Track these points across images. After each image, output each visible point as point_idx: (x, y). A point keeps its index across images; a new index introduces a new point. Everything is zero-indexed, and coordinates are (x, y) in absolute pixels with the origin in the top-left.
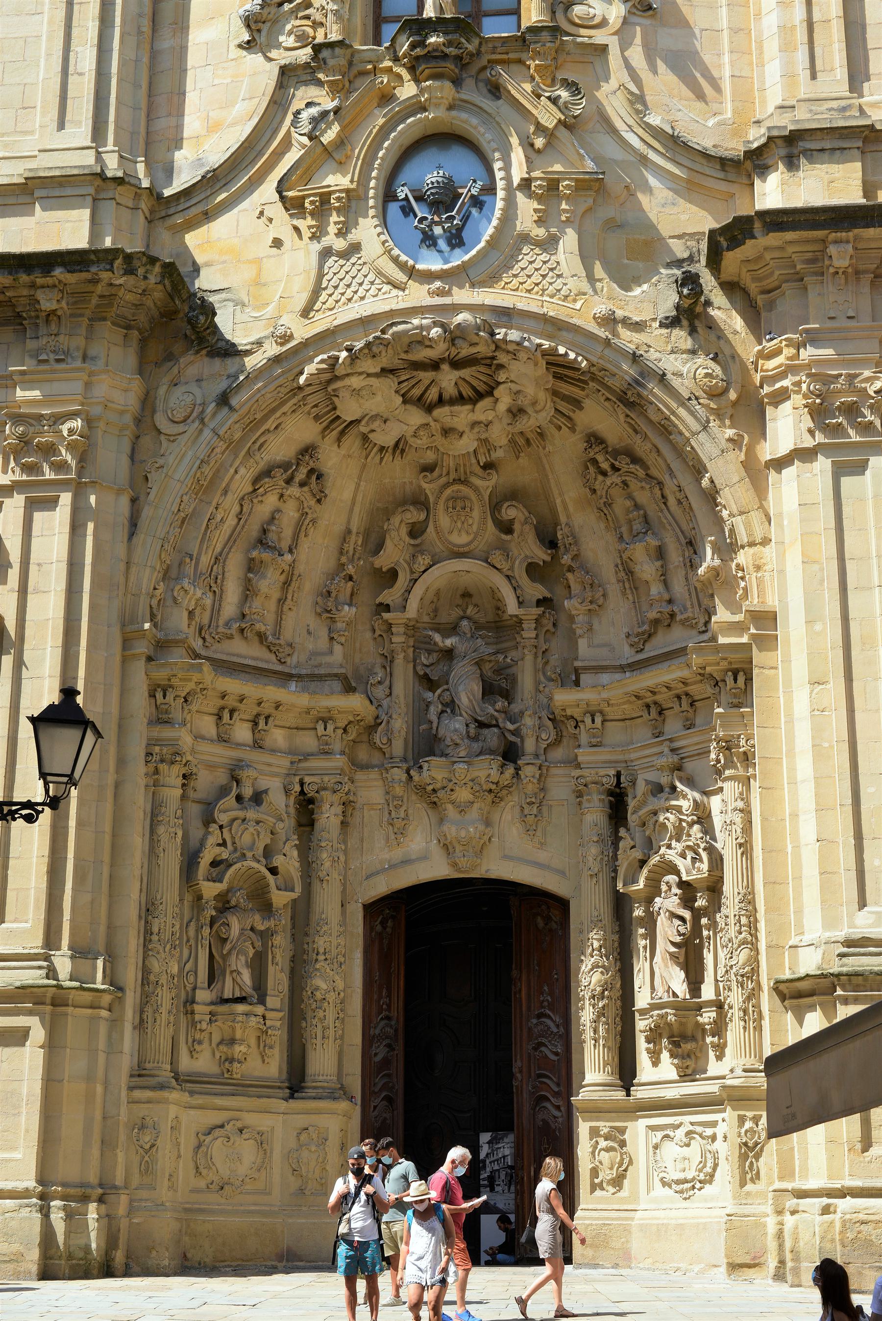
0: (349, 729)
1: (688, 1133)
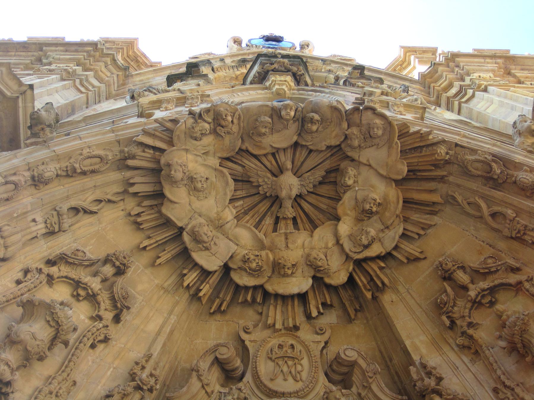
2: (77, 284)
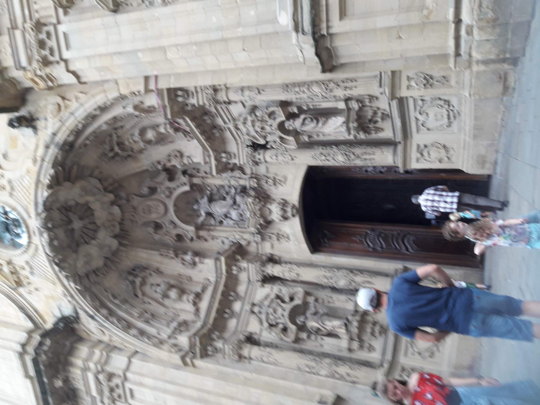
1: (420, 114)
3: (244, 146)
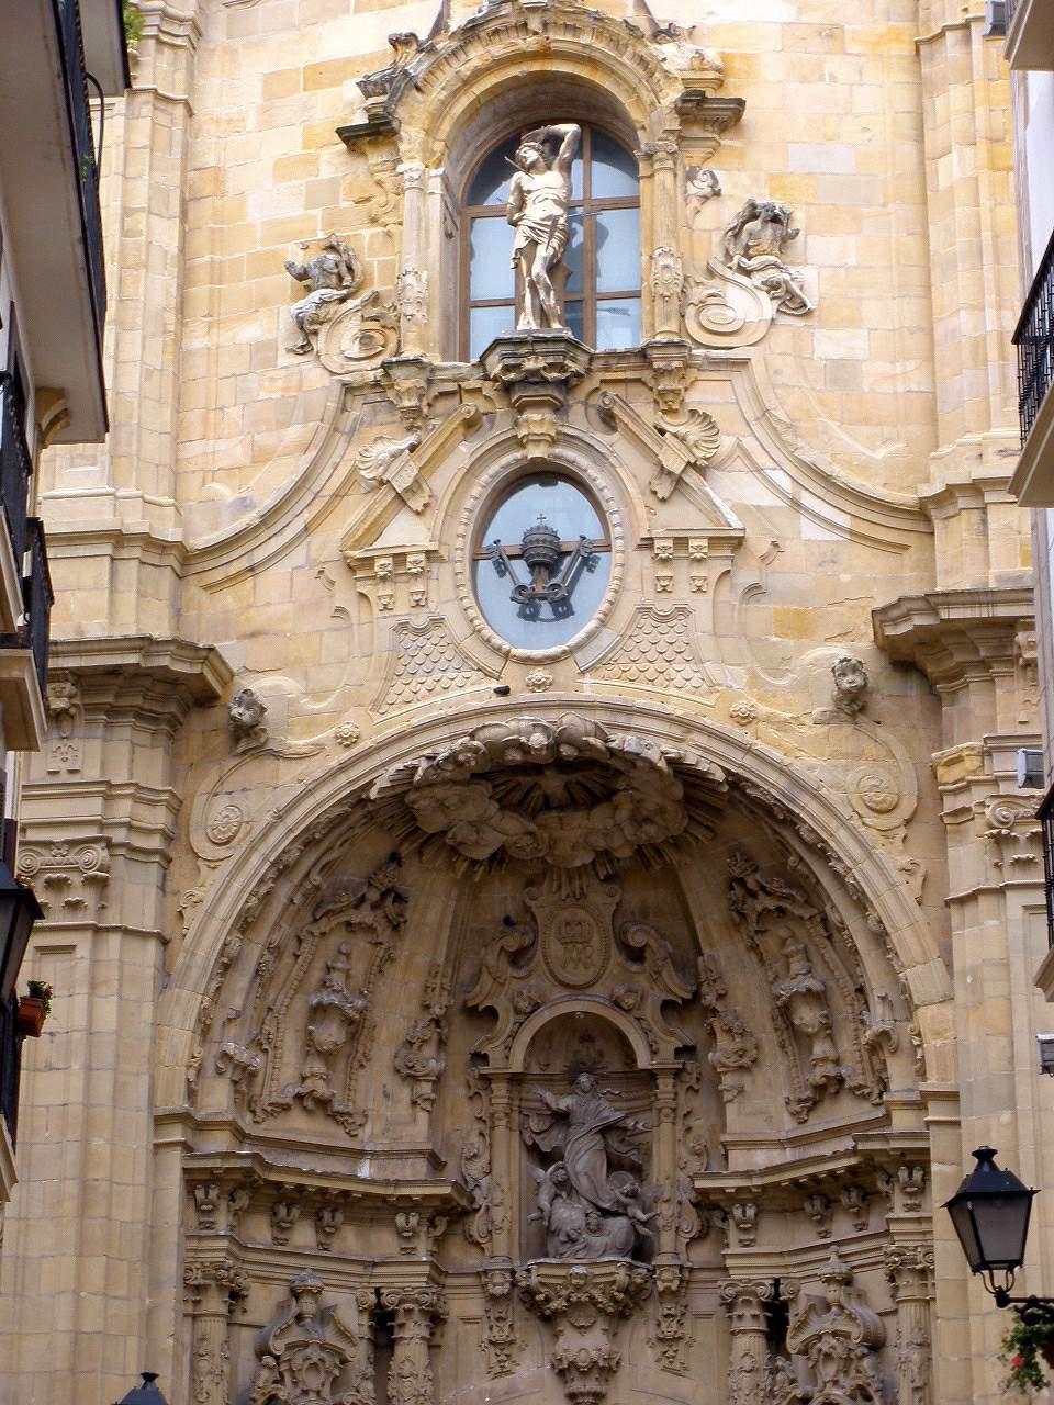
0: (438, 1221)
2: (348, 924)
3: (777, 1273)
